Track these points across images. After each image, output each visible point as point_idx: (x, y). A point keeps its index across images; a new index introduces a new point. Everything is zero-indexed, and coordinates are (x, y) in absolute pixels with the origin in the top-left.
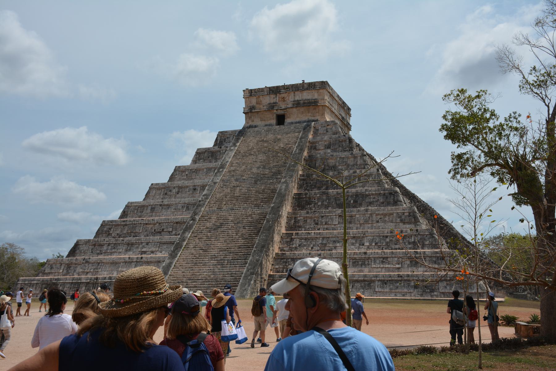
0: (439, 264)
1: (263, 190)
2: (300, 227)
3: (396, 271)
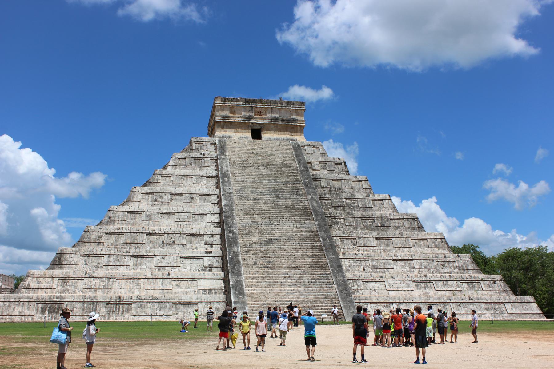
0: (493, 288)
1: (293, 205)
3: (459, 293)
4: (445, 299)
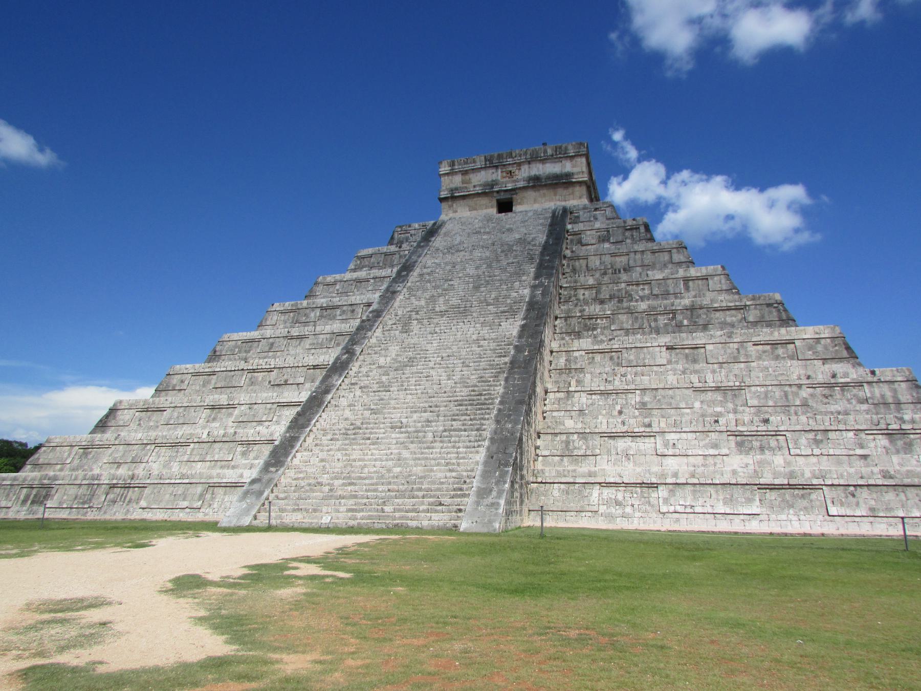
1: (496, 299)
2: (581, 370)
4: (808, 474)
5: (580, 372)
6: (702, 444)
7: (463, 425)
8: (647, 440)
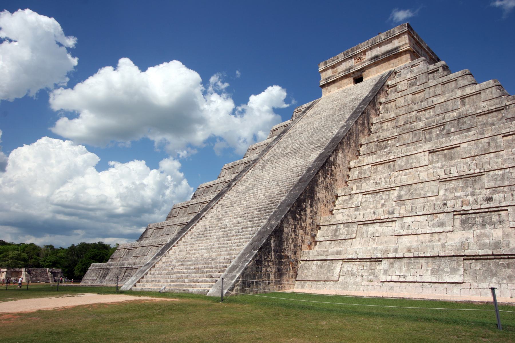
5: (367, 180)
6: (431, 223)
7: (253, 224)
8: (390, 224)
